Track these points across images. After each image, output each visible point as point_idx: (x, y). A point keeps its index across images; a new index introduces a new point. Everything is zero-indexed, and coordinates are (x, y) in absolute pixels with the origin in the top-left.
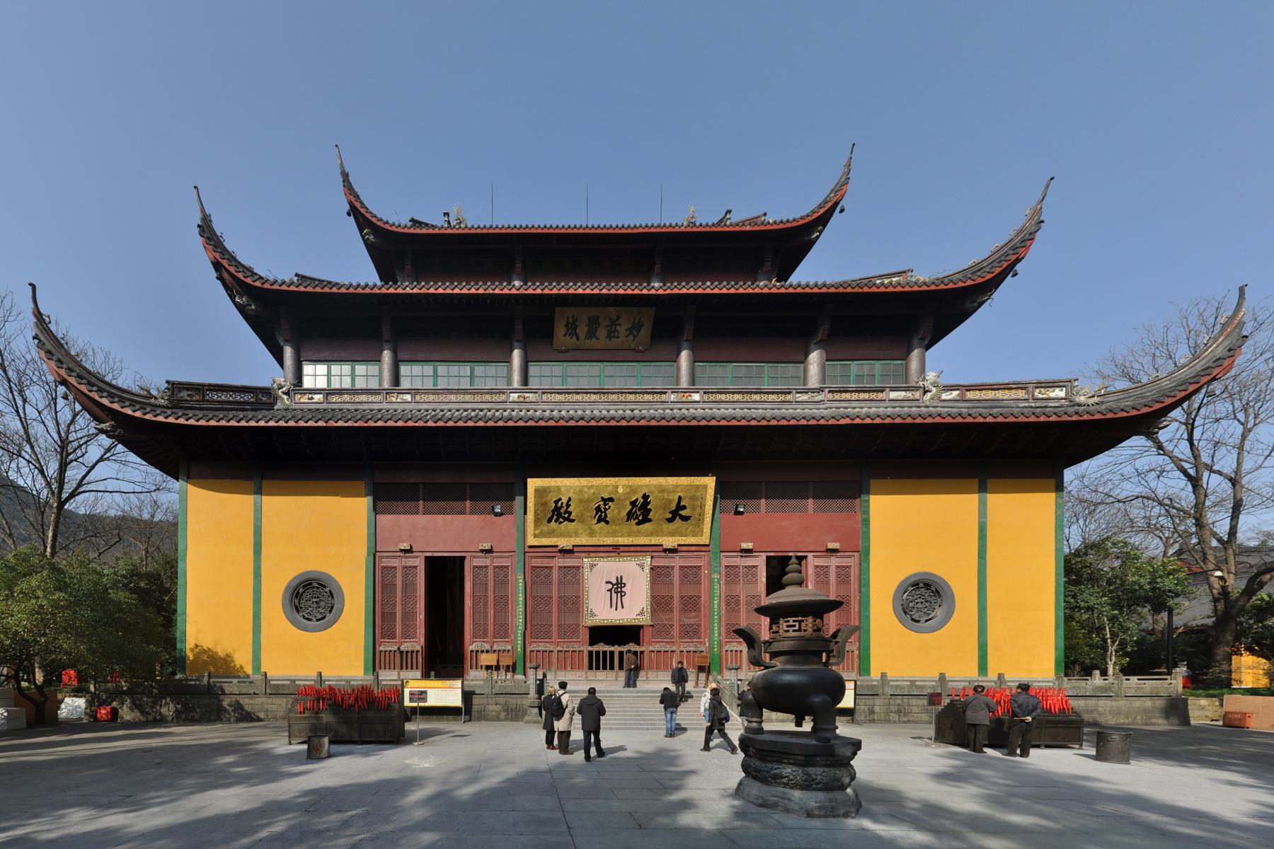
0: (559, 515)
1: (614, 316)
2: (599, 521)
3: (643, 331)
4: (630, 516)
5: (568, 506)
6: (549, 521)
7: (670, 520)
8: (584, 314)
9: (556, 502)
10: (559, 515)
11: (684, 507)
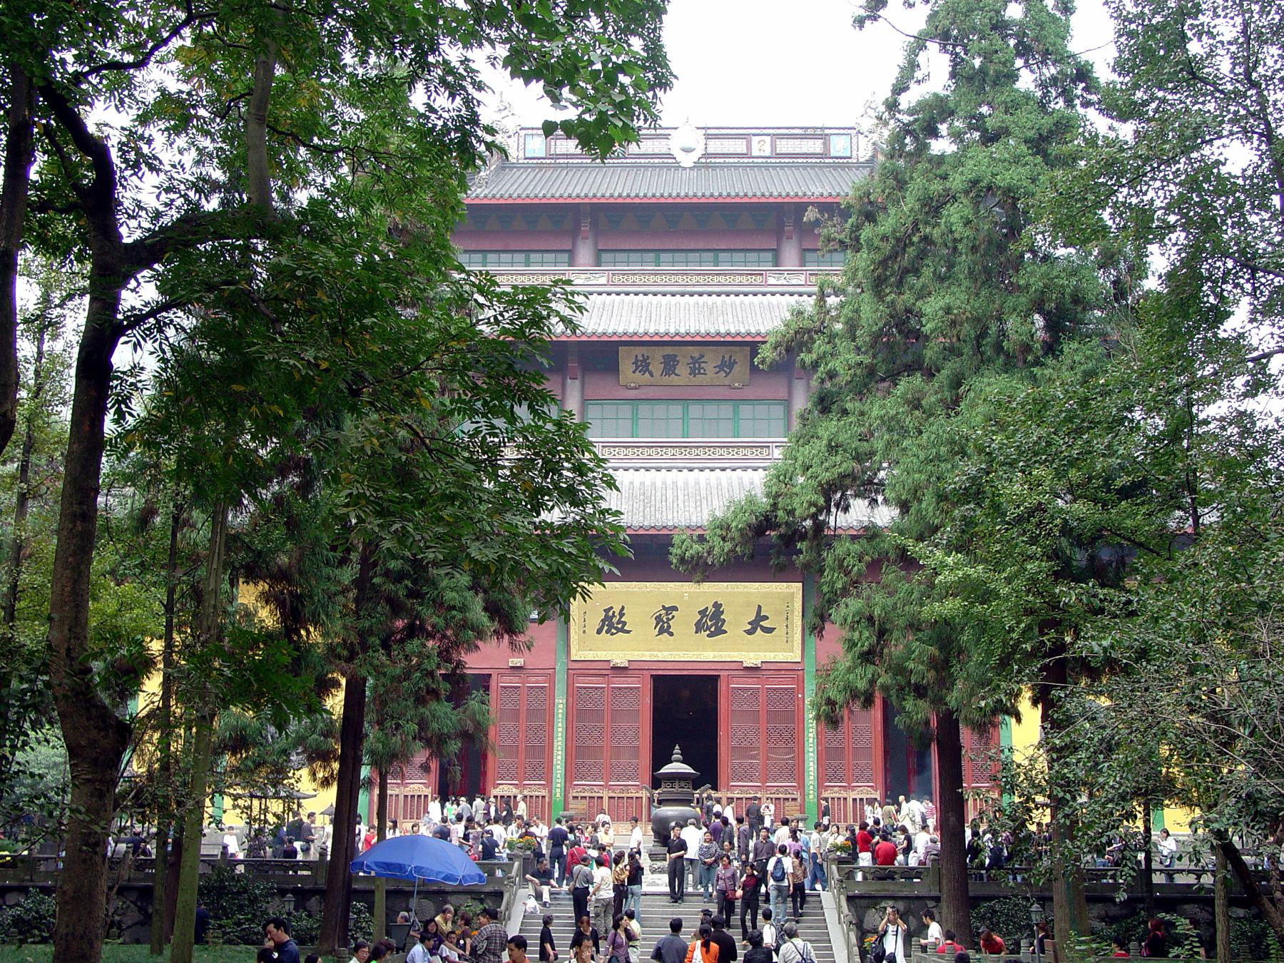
0: (611, 626)
1: (696, 355)
2: (660, 633)
3: (737, 368)
4: (699, 627)
5: (621, 614)
6: (599, 632)
7: (749, 632)
9: (607, 611)
10: (611, 626)
11: (766, 618)
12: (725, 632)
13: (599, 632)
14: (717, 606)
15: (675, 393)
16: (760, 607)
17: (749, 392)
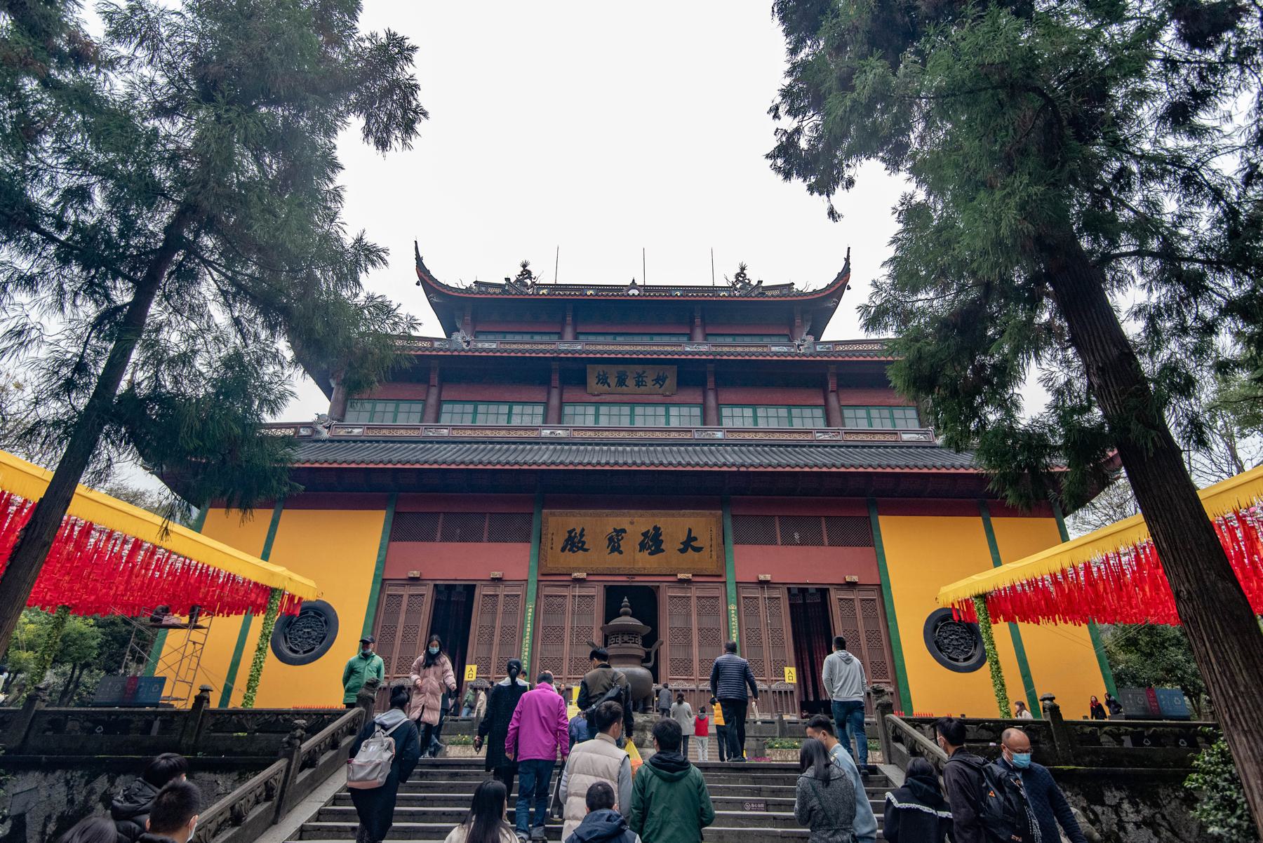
0: (573, 544)
2: (612, 551)
3: (667, 382)
4: (643, 546)
5: (582, 535)
6: (563, 550)
7: (682, 551)
8: (612, 372)
9: (570, 532)
10: (573, 544)
11: (695, 539)
12: (663, 551)
13: (563, 550)
14: (656, 529)
15: (625, 398)
16: (690, 530)
17: (676, 399)
